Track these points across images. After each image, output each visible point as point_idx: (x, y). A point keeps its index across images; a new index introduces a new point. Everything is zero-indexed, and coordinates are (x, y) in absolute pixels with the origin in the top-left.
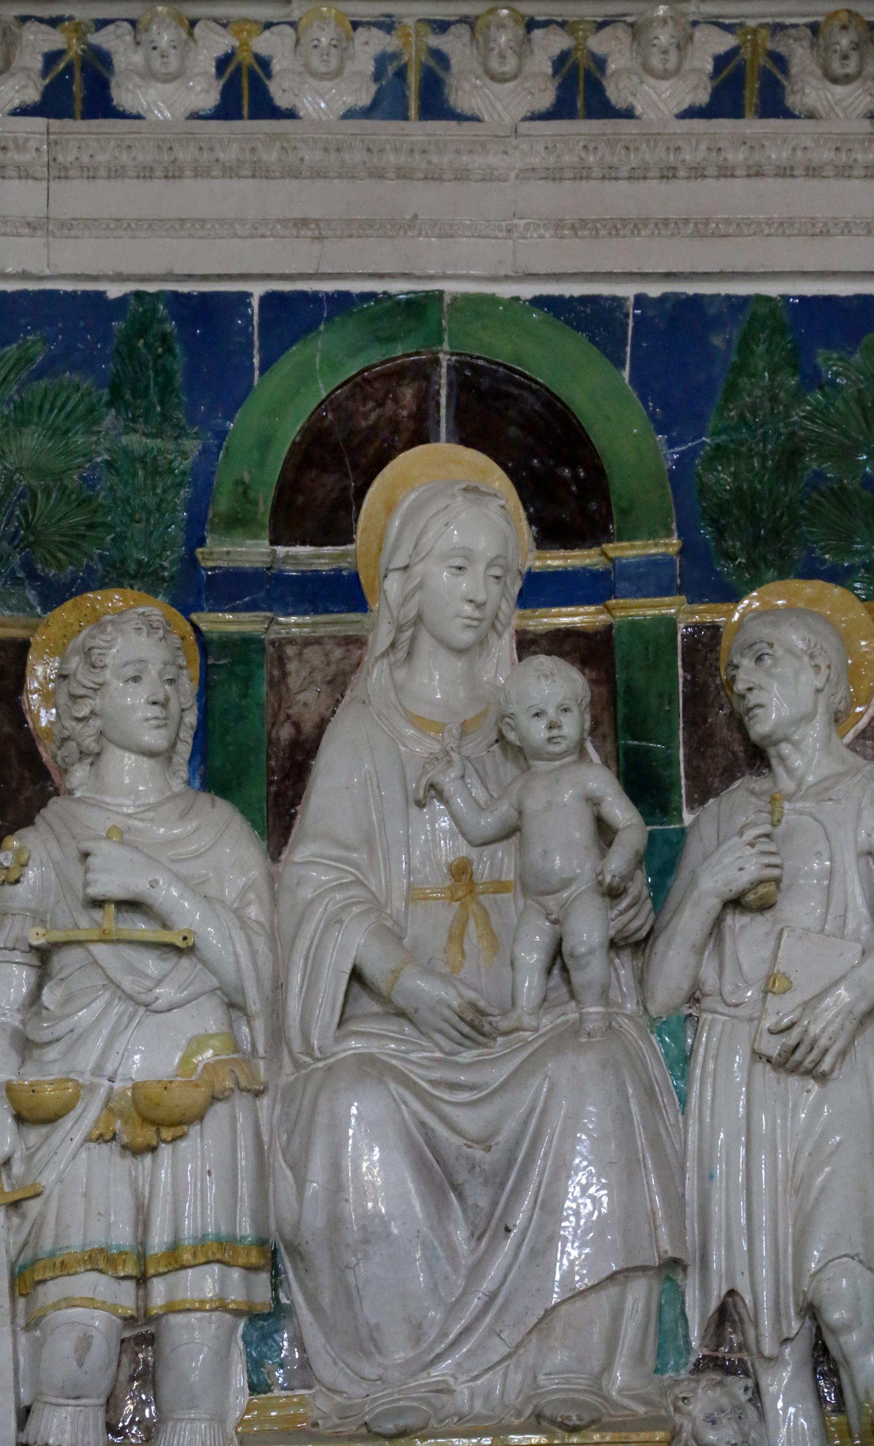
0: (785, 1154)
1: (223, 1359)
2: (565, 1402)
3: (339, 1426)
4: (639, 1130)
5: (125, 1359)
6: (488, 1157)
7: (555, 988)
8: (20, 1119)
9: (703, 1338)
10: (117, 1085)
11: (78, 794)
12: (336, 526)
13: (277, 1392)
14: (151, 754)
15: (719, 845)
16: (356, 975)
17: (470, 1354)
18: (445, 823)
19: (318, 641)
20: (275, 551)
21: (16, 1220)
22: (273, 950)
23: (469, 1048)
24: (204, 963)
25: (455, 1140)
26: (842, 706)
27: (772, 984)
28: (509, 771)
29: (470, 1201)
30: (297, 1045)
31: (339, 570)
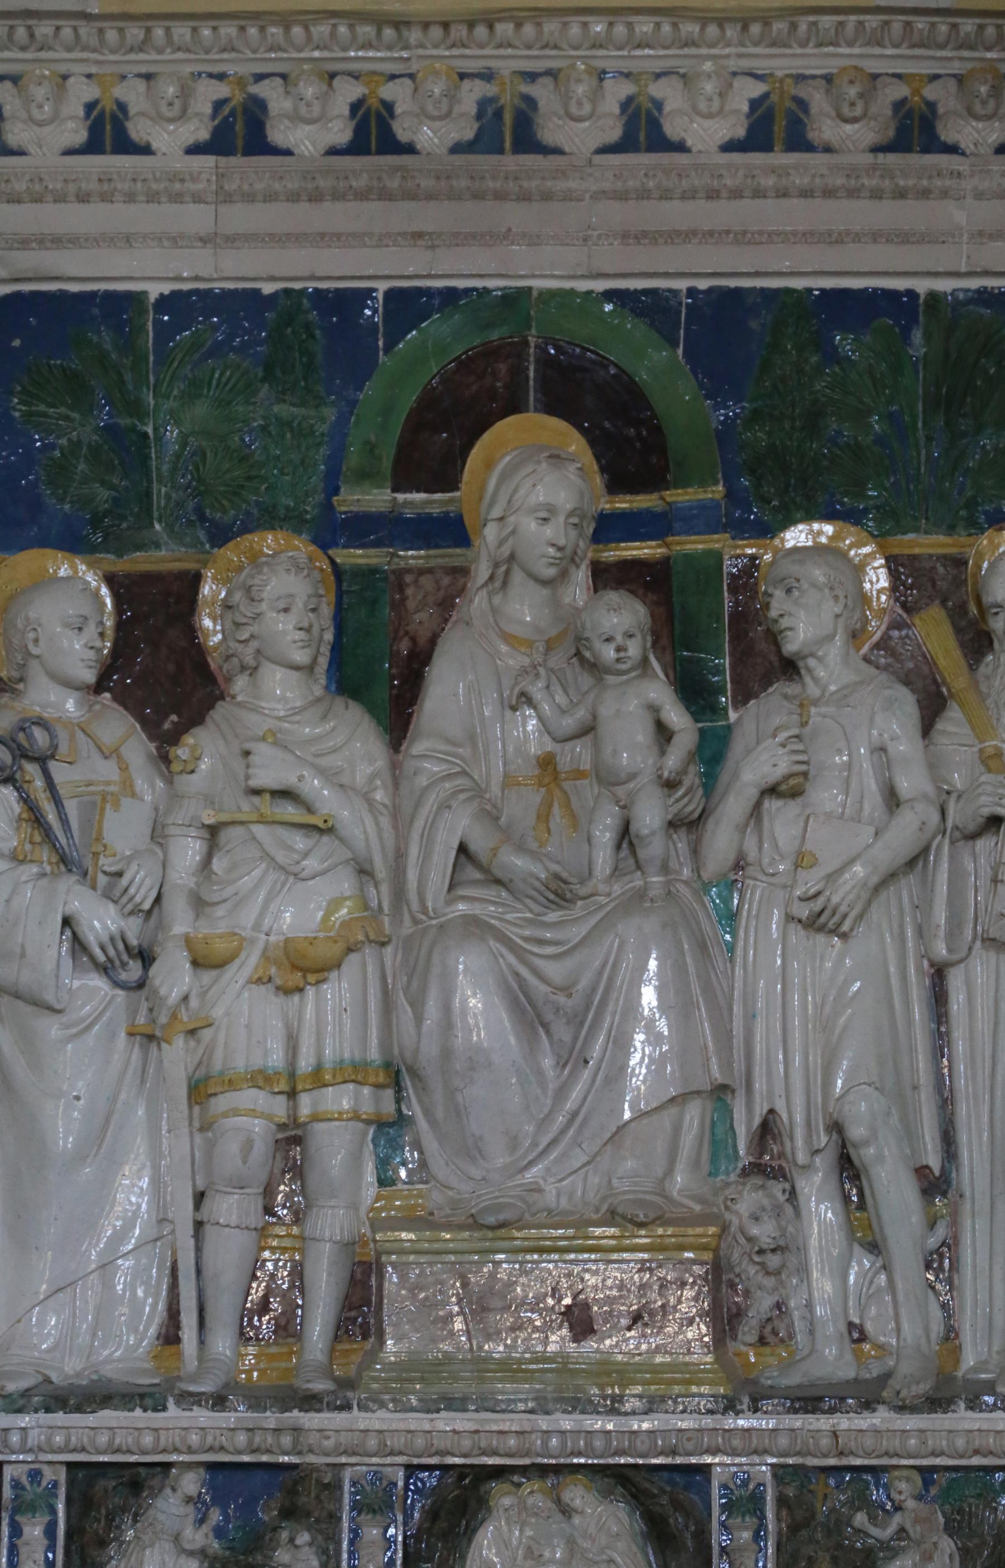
0: (814, 998)
1: (356, 1159)
2: (634, 1201)
3: (452, 1215)
4: (693, 978)
5: (278, 1156)
6: (570, 1003)
7: (624, 859)
8: (195, 963)
9: (748, 1148)
10: (272, 938)
11: (239, 698)
12: (446, 477)
13: (400, 1186)
14: (297, 668)
15: (758, 742)
16: (463, 849)
17: (557, 1161)
18: (532, 724)
19: (430, 571)
20: (395, 499)
21: (192, 1044)
22: (395, 827)
23: (554, 910)
24: (341, 840)
25: (543, 988)
26: (858, 626)
27: (802, 860)
28: (586, 681)
29: (556, 1038)
30: (415, 906)
31: (447, 513)
